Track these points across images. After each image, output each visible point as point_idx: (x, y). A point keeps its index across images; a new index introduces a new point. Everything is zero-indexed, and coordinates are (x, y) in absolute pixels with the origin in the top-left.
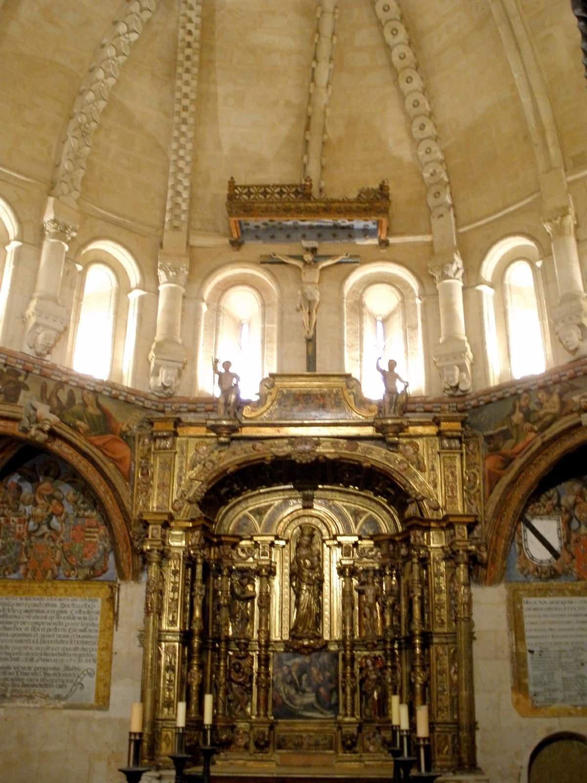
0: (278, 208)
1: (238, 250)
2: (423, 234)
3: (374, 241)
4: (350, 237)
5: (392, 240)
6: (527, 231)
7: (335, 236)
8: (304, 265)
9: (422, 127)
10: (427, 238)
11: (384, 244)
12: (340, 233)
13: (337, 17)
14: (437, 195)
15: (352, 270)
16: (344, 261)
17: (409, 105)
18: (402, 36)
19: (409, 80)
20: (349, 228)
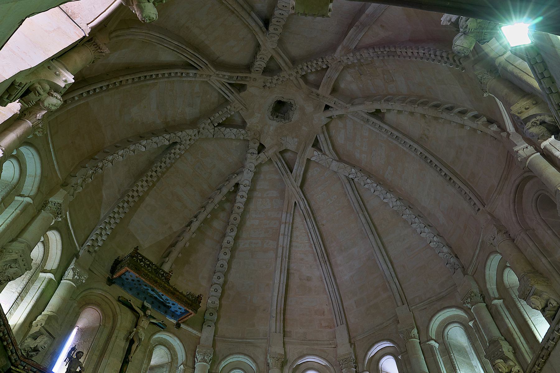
0: (152, 277)
1: (110, 286)
2: (197, 331)
3: (174, 322)
4: (166, 312)
5: (182, 326)
6: (252, 356)
7: (159, 307)
8: (144, 316)
9: (219, 278)
10: (199, 335)
11: (178, 326)
12: (162, 307)
13: (216, 207)
14: (212, 314)
15: (159, 331)
16: (160, 324)
17: (218, 265)
18: (234, 234)
19: (225, 254)
20: (169, 307)
